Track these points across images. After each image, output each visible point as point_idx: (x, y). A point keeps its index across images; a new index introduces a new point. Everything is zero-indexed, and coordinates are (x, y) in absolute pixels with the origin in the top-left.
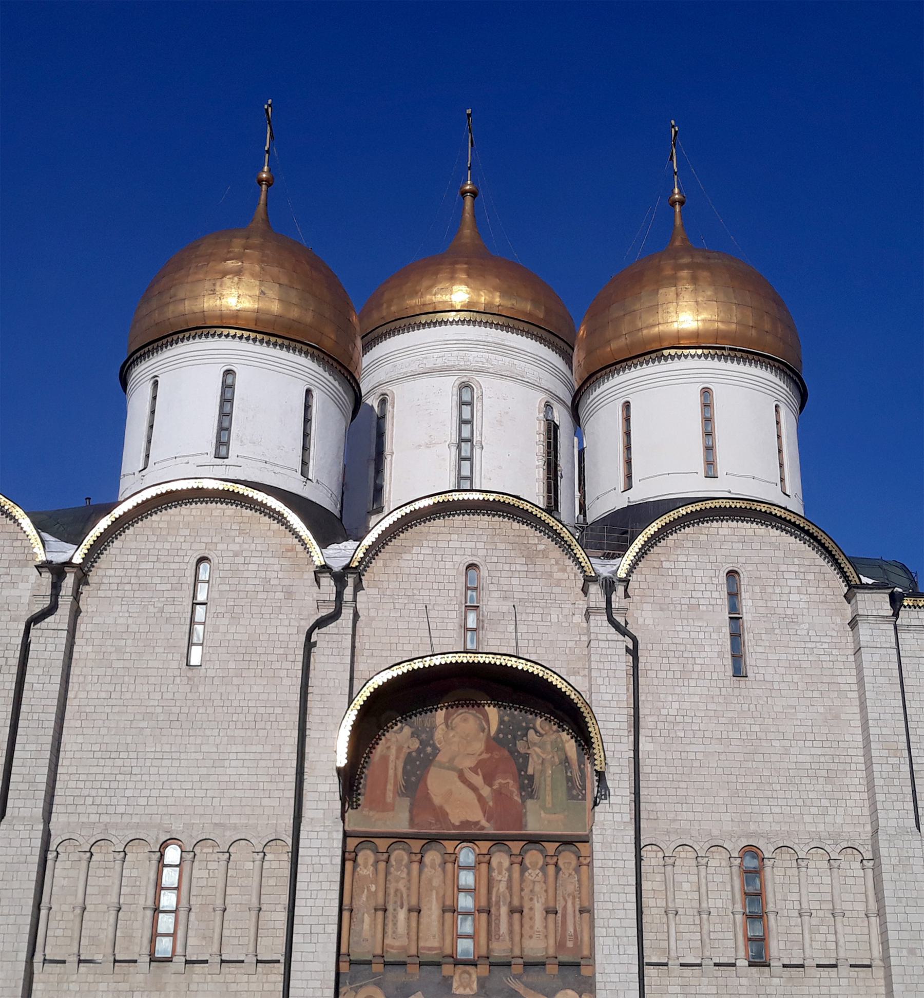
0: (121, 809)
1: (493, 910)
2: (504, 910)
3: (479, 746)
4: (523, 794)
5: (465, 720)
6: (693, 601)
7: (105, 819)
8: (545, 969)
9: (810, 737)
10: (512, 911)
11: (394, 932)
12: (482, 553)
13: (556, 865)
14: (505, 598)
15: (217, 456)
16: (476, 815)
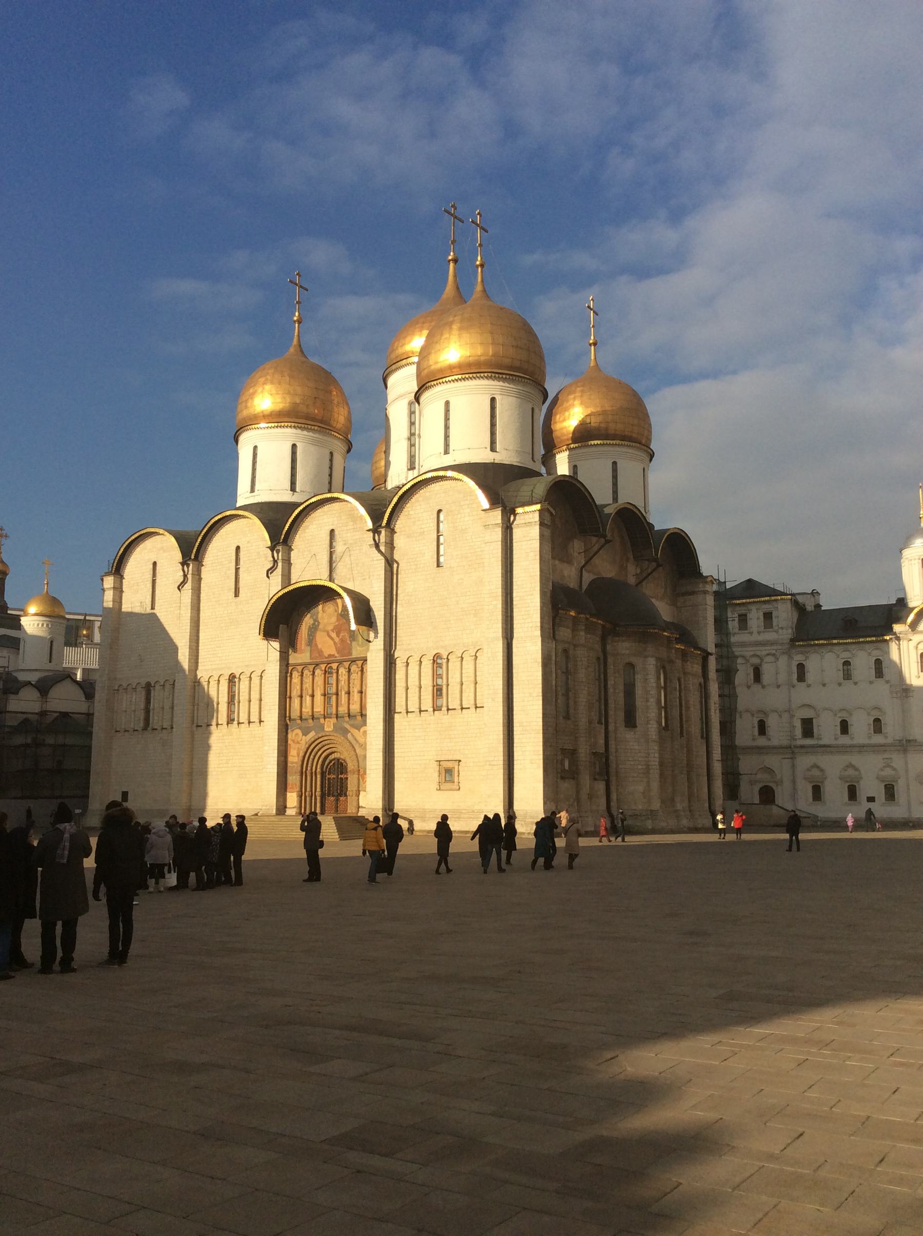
0: (218, 662)
1: (339, 693)
2: (343, 693)
3: (334, 619)
4: (351, 639)
5: (329, 607)
6: (422, 530)
7: (214, 667)
8: (356, 718)
9: (469, 594)
10: (345, 693)
11: (305, 706)
12: (336, 523)
13: (362, 670)
14: (345, 544)
15: (251, 492)
16: (333, 651)
